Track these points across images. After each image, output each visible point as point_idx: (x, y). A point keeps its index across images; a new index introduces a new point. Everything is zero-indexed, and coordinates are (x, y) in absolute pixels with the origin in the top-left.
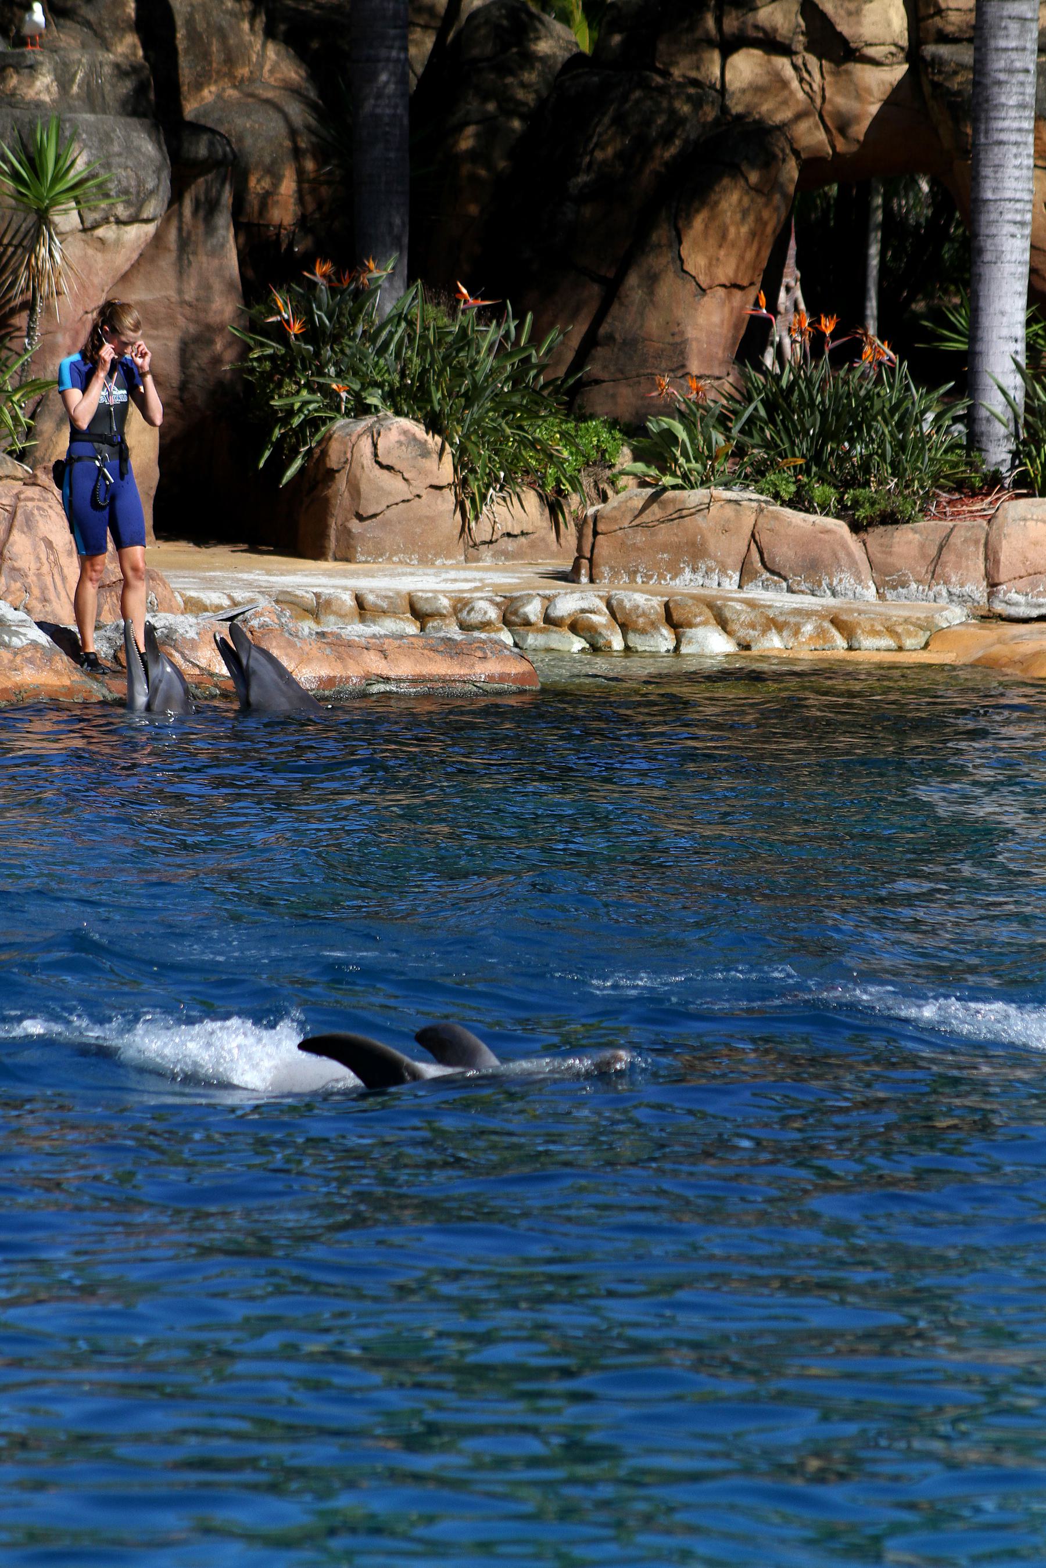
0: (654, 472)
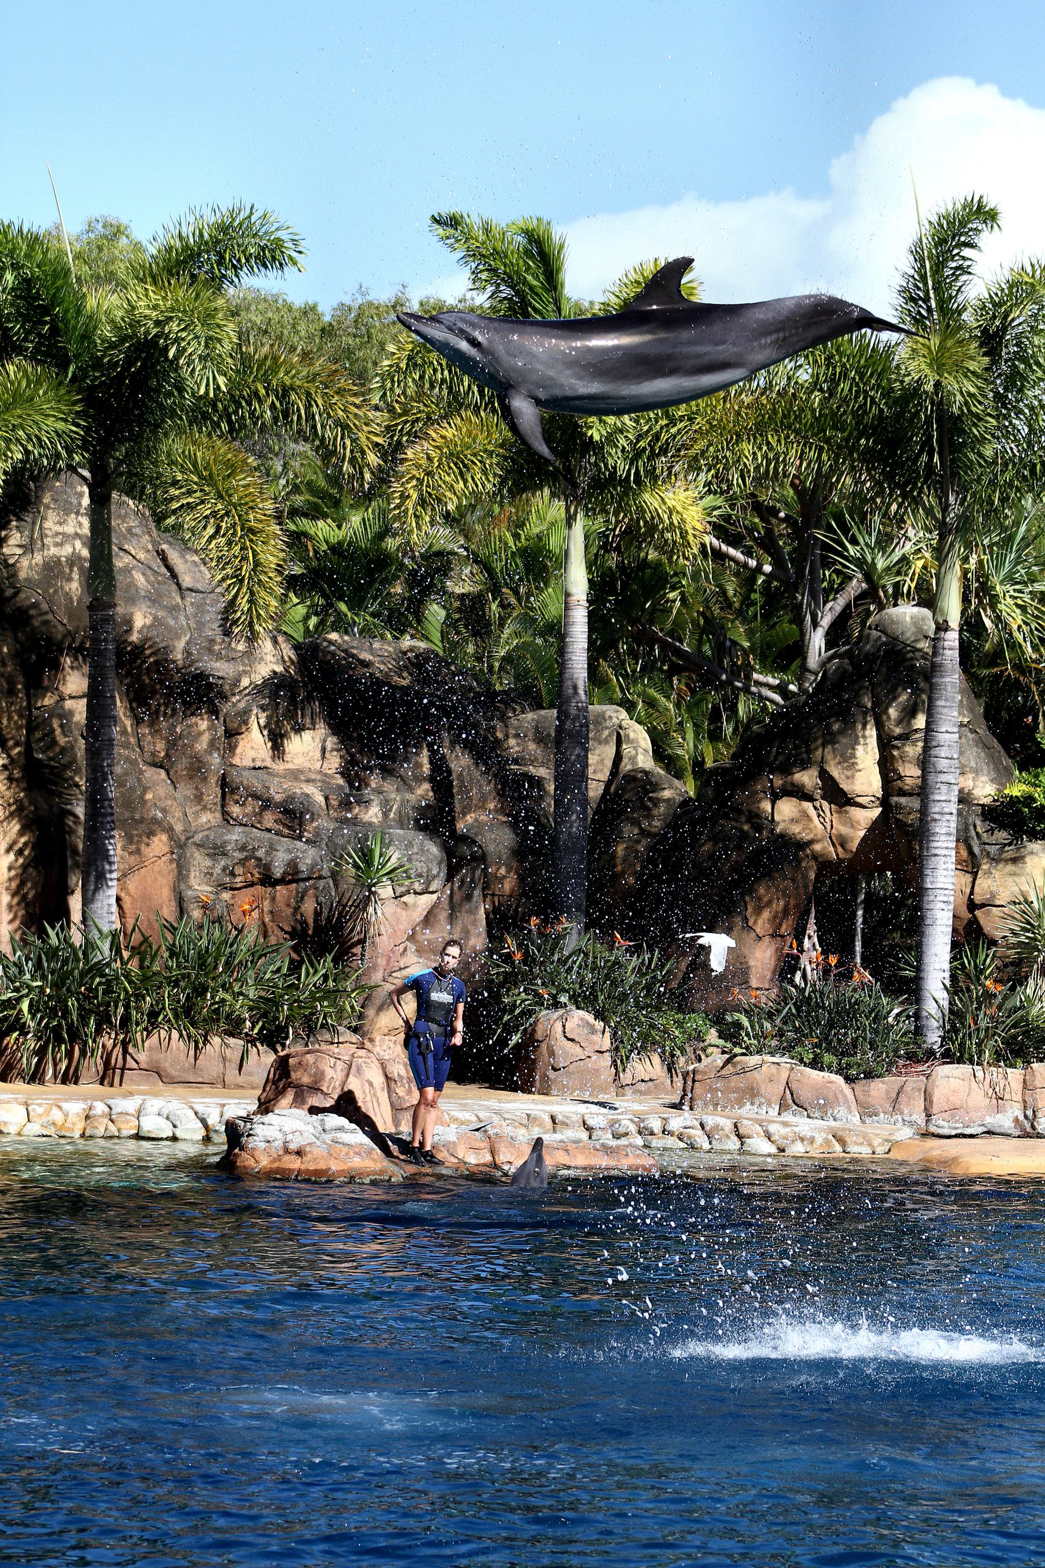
0: (729, 1045)
